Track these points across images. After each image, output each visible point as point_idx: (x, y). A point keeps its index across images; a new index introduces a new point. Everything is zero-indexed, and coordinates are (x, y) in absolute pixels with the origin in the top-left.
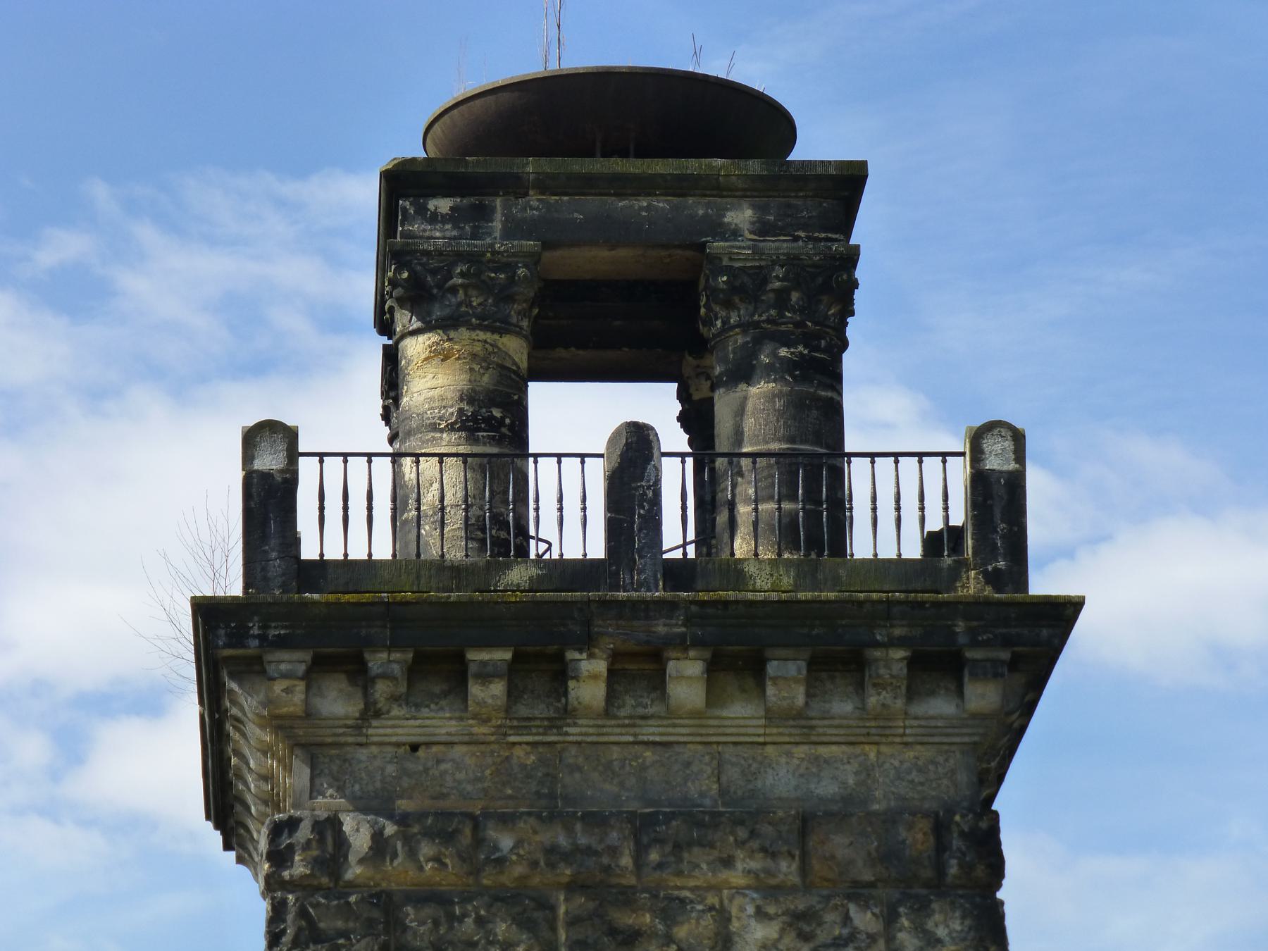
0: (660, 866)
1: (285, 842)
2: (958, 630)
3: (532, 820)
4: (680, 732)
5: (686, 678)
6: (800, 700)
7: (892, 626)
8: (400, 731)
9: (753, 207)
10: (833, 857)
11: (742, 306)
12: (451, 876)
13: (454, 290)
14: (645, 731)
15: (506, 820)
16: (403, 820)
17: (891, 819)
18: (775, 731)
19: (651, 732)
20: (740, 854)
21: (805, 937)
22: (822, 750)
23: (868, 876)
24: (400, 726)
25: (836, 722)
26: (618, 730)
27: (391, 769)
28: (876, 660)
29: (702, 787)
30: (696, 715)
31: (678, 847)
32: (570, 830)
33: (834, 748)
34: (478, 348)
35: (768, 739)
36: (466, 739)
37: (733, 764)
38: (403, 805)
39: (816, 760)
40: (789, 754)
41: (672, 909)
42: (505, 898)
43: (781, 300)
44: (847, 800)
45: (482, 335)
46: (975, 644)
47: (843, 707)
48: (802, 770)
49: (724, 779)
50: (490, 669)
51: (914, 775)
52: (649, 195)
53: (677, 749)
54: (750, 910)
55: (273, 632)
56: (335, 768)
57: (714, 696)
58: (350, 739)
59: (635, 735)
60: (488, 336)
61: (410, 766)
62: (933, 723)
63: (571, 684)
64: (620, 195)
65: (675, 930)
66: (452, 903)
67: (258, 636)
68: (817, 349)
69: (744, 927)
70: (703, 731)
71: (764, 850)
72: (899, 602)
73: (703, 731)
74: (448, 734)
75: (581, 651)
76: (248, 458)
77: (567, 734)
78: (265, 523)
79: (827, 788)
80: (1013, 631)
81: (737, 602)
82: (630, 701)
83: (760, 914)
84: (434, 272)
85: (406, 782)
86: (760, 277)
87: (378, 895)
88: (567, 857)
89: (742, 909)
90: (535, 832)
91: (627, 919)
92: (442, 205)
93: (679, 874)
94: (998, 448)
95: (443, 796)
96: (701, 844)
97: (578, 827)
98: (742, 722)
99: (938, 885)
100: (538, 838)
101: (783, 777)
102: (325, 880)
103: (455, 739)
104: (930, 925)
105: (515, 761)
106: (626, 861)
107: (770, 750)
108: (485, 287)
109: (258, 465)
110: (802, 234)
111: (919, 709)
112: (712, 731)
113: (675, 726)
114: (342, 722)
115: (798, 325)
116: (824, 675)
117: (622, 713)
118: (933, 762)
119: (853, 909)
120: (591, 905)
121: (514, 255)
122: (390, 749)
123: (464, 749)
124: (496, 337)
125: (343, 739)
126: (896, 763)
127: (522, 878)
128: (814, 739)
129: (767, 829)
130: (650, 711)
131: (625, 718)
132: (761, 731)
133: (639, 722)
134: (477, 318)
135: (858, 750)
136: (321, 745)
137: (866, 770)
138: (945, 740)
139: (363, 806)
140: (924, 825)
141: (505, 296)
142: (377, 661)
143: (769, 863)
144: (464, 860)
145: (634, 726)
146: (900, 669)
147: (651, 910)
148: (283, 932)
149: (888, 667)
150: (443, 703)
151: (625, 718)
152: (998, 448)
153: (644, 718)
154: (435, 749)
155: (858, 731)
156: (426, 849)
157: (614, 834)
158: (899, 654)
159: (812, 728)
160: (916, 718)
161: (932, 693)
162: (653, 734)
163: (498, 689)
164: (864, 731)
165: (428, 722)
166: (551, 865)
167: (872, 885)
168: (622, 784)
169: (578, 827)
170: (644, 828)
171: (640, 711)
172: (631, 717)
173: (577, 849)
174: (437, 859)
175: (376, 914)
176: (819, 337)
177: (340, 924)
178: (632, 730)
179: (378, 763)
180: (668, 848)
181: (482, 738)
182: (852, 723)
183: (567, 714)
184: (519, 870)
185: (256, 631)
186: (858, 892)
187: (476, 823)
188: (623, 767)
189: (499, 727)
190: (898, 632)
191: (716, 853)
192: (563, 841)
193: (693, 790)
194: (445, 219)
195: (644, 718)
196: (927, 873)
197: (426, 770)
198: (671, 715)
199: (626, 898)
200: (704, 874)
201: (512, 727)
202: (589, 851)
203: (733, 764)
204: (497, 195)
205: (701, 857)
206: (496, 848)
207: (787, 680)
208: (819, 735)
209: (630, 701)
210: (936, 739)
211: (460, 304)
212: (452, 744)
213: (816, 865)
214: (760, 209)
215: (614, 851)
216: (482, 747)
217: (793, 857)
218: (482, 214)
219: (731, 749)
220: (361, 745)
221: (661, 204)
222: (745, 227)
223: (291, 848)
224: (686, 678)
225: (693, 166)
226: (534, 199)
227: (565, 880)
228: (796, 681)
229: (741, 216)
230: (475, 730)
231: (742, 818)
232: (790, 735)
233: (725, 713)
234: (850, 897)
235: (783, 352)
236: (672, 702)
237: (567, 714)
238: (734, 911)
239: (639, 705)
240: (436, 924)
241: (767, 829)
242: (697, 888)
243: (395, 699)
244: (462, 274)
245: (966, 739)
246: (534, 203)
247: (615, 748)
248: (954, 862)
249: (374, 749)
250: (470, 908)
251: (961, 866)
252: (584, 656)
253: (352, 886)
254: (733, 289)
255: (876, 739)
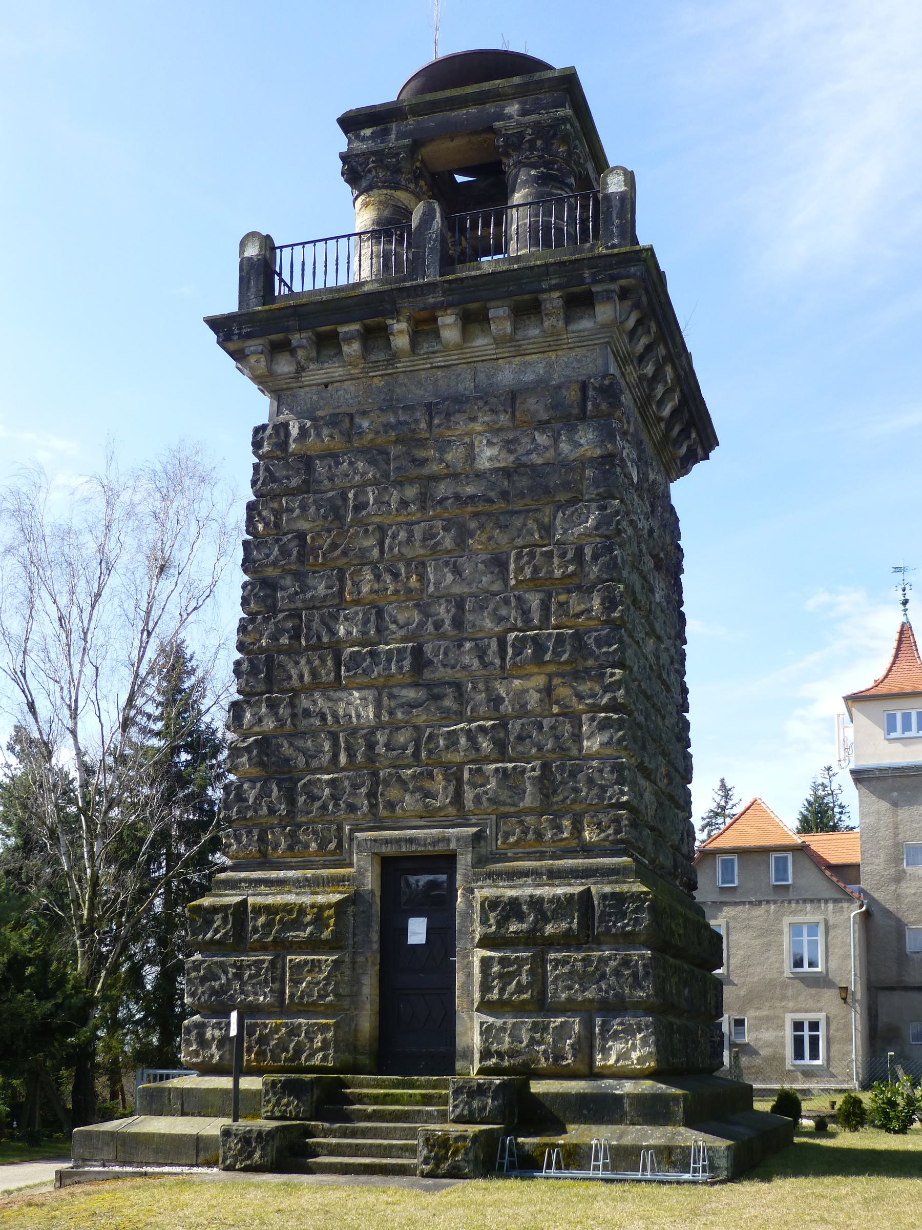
0: (439, 426)
1: (260, 436)
2: (585, 276)
3: (377, 412)
4: (453, 358)
5: (449, 328)
6: (509, 329)
7: (550, 279)
8: (316, 377)
9: (519, 103)
10: (528, 410)
11: (514, 154)
12: (338, 444)
13: (370, 171)
14: (435, 360)
15: (364, 413)
16: (314, 419)
17: (559, 387)
18: (501, 350)
19: (439, 360)
20: (480, 414)
21: (511, 452)
22: (527, 358)
23: (545, 417)
24: (316, 374)
25: (531, 341)
26: (421, 362)
27: (315, 397)
28: (545, 300)
29: (466, 385)
30: (458, 347)
31: (448, 415)
32: (396, 414)
33: (534, 356)
34: (383, 198)
35: (498, 356)
36: (349, 377)
37: (482, 372)
38: (320, 413)
39: (524, 363)
40: (510, 363)
41: (444, 446)
42: (363, 452)
43: (533, 147)
44: (539, 382)
45: (384, 191)
46: (595, 282)
47: (534, 332)
48: (517, 370)
49: (477, 380)
50: (349, 335)
51: (575, 364)
52: (466, 107)
53: (454, 368)
54: (485, 442)
55: (244, 331)
56: (289, 401)
57: (466, 335)
58: (294, 385)
59: (431, 363)
60: (388, 192)
61: (324, 395)
62: (582, 334)
63: (391, 338)
64: (452, 110)
65: (445, 456)
66: (338, 457)
67: (238, 334)
68: (553, 169)
69: (481, 451)
70: (464, 356)
71: (492, 410)
72: (552, 264)
73: (464, 356)
74: (340, 376)
75: (393, 319)
76: (242, 251)
77: (397, 368)
78: (249, 282)
79: (529, 377)
80: (615, 271)
81: (467, 278)
82: (426, 345)
83: (490, 443)
84: (361, 165)
85: (322, 403)
86: (521, 135)
87: (302, 457)
88: (393, 427)
89: (481, 442)
90: (378, 417)
91: (421, 454)
92: (367, 132)
93: (449, 428)
94: (615, 180)
95: (339, 407)
96: (459, 412)
97: (400, 412)
98: (483, 348)
99: (583, 417)
100: (380, 420)
101: (506, 375)
102: (279, 453)
103: (344, 378)
104: (577, 438)
105: (374, 386)
106: (423, 425)
107: (500, 361)
108: (386, 167)
109: (246, 254)
110: (543, 112)
111: (574, 327)
112: (468, 355)
113: (450, 355)
114: (287, 376)
115: (539, 157)
116: (525, 317)
117: (422, 352)
118: (585, 357)
119: (537, 434)
120: (404, 449)
121: (399, 148)
122: (314, 388)
123: (350, 382)
124: (393, 191)
125: (291, 385)
126: (566, 360)
127: (372, 440)
128: (523, 352)
129: (493, 400)
130: (436, 348)
131: (424, 354)
132: (494, 352)
133: (431, 356)
134: (381, 182)
135: (546, 354)
136: (283, 390)
137: (550, 365)
138: (590, 343)
139: (300, 416)
140: (576, 387)
141: (397, 170)
142: (296, 339)
143: (494, 417)
144: (344, 435)
145: (429, 358)
146: (559, 303)
147: (434, 448)
148: (258, 479)
149: (551, 303)
150: (335, 359)
151: (424, 354)
152: (615, 180)
153: (433, 353)
154: (335, 385)
155: (544, 344)
156: (325, 431)
157: (418, 413)
158: (556, 294)
159: (520, 346)
160: (573, 332)
161: (581, 318)
162: (439, 362)
163: (356, 346)
164: (547, 344)
165: (329, 370)
166: (386, 432)
167: (548, 422)
168: (425, 390)
169: (400, 412)
170: (430, 409)
171: (431, 349)
172: (426, 353)
173: (399, 423)
174: (331, 436)
175: (301, 466)
176: (553, 163)
177: (285, 473)
178: (428, 361)
179: (309, 395)
180: (443, 416)
181: (357, 376)
182: (540, 340)
183: (394, 357)
184: (370, 436)
185: (236, 332)
186: (542, 426)
187: (351, 416)
188: (426, 381)
189: (363, 368)
190: (554, 282)
191: (467, 415)
192: (392, 420)
193: (461, 387)
194: (369, 138)
195: (433, 353)
196: (575, 411)
197: (332, 396)
198: (446, 349)
199: (422, 443)
200: (462, 428)
201: (370, 368)
202: (405, 423)
203: (482, 372)
204: (393, 122)
205: (458, 417)
206: (360, 427)
207: (500, 319)
208: (524, 350)
209: (426, 345)
210: (586, 343)
211: (373, 178)
212: (343, 381)
213: (518, 414)
214: (522, 103)
215: (417, 421)
216: (358, 381)
217: (507, 413)
218: (386, 132)
219: (480, 364)
220: (301, 387)
221: (473, 110)
222: (515, 114)
223: (262, 438)
224: (449, 328)
225: (486, 86)
226: (411, 120)
227: (393, 439)
228: (505, 318)
229: (513, 109)
230: (352, 372)
231: (485, 397)
232: (509, 352)
233: (474, 344)
234: (535, 429)
235: (533, 172)
236: (443, 340)
237: (394, 357)
238: (476, 443)
239: (430, 346)
240: (330, 467)
241: (493, 400)
242: (460, 435)
243: (309, 359)
244: (373, 162)
245: (602, 341)
246: (411, 122)
247: (423, 372)
248: (590, 403)
249: (307, 388)
250: (346, 457)
251: (593, 405)
252: (395, 321)
253: (292, 454)
254: (507, 144)
255: (554, 348)
